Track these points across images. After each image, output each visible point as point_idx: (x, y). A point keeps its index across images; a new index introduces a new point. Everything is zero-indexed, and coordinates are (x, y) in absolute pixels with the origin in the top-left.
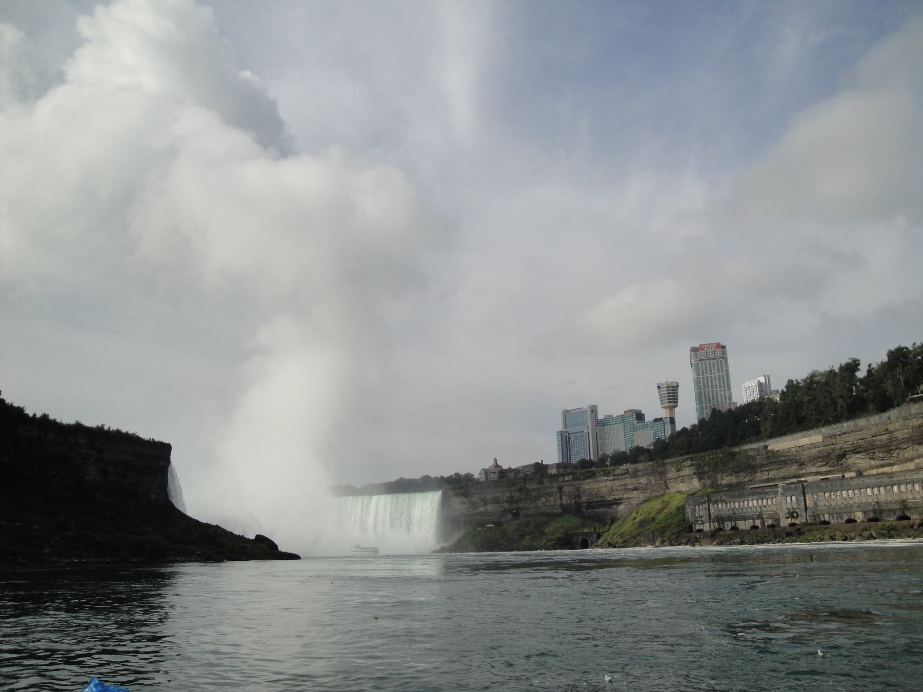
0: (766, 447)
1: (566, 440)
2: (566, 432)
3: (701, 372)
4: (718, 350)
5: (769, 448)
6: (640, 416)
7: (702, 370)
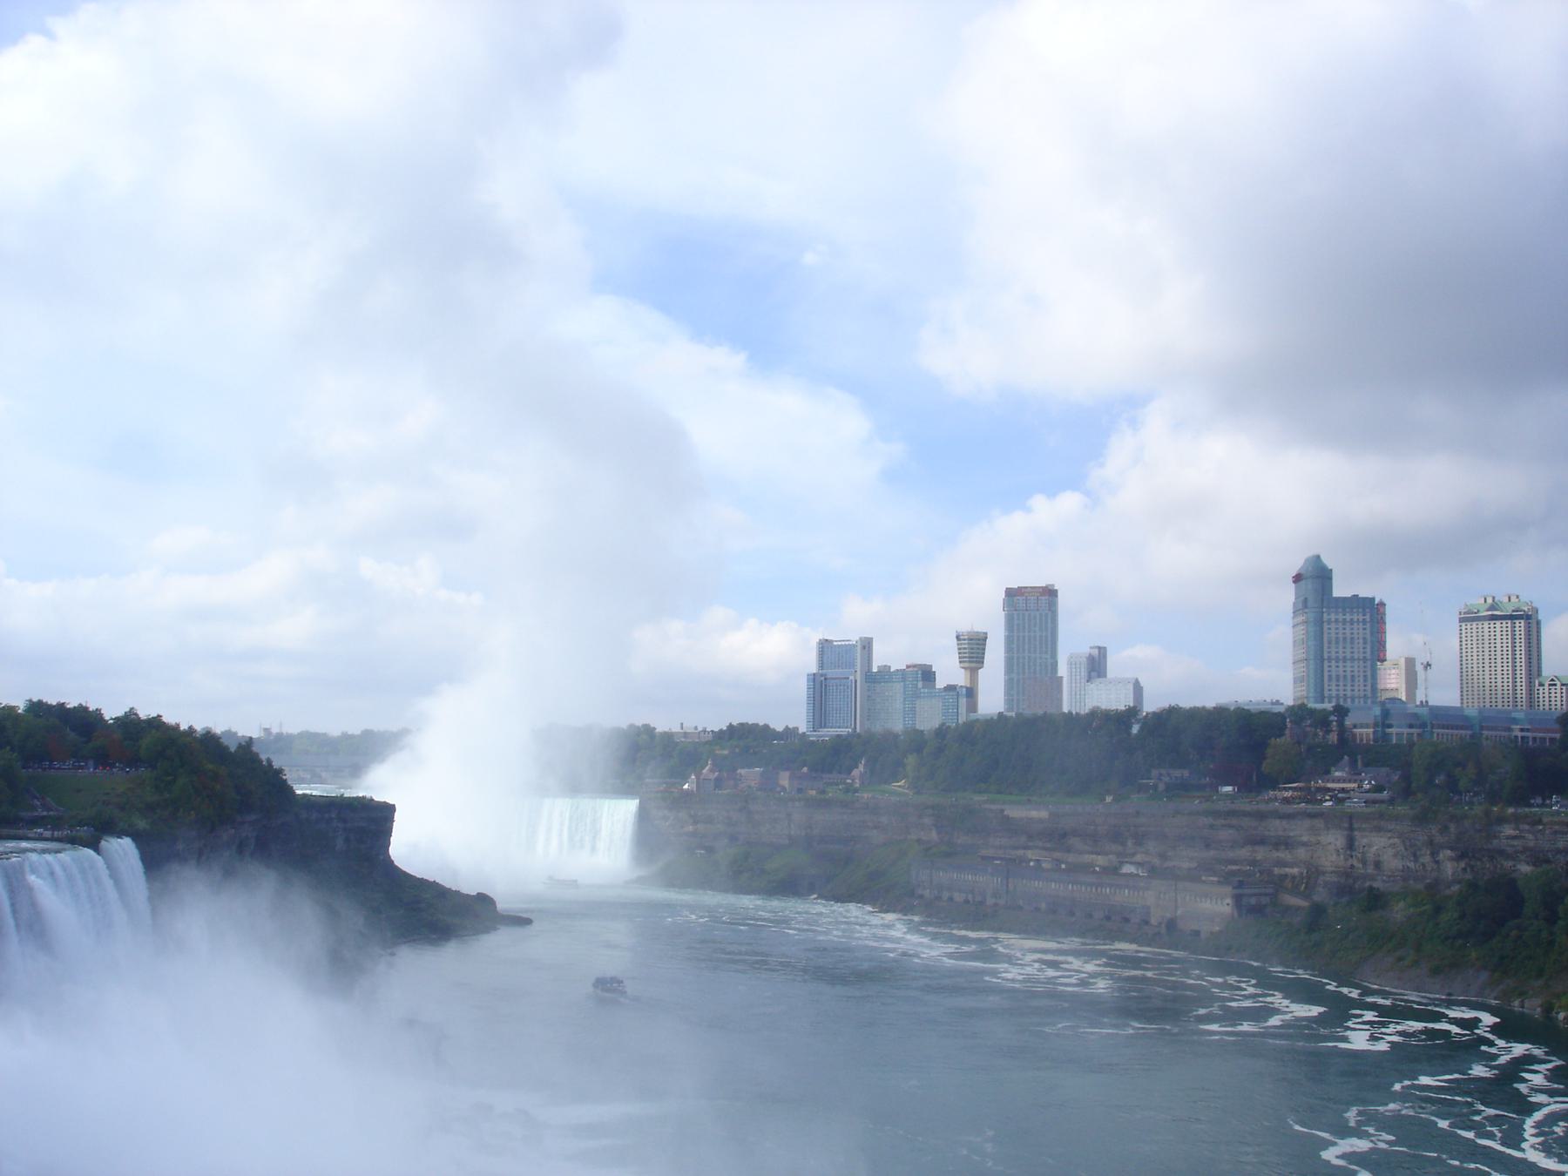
0: (1002, 811)
1: (820, 688)
2: (822, 675)
3: (1015, 627)
4: (1043, 598)
5: (1006, 813)
6: (927, 674)
7: (1018, 625)
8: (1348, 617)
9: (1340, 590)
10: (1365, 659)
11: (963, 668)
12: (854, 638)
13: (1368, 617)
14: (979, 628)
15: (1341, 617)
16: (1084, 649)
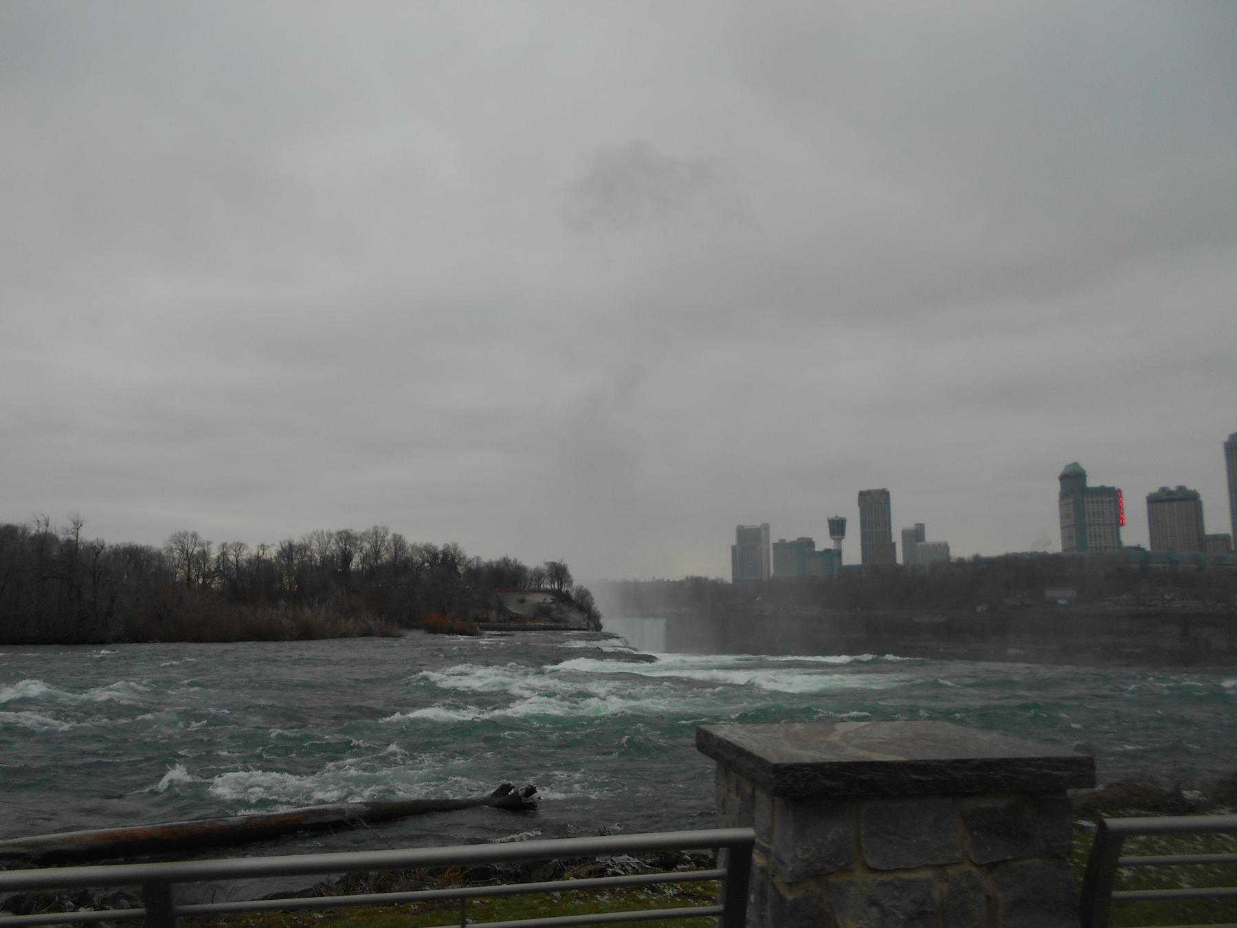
6: (810, 543)
8: (1099, 499)
9: (1092, 482)
10: (1111, 524)
11: (834, 539)
12: (758, 524)
13: (1112, 499)
14: (841, 515)
15: (1094, 499)
16: (910, 525)
